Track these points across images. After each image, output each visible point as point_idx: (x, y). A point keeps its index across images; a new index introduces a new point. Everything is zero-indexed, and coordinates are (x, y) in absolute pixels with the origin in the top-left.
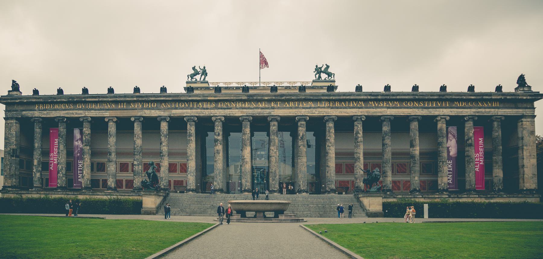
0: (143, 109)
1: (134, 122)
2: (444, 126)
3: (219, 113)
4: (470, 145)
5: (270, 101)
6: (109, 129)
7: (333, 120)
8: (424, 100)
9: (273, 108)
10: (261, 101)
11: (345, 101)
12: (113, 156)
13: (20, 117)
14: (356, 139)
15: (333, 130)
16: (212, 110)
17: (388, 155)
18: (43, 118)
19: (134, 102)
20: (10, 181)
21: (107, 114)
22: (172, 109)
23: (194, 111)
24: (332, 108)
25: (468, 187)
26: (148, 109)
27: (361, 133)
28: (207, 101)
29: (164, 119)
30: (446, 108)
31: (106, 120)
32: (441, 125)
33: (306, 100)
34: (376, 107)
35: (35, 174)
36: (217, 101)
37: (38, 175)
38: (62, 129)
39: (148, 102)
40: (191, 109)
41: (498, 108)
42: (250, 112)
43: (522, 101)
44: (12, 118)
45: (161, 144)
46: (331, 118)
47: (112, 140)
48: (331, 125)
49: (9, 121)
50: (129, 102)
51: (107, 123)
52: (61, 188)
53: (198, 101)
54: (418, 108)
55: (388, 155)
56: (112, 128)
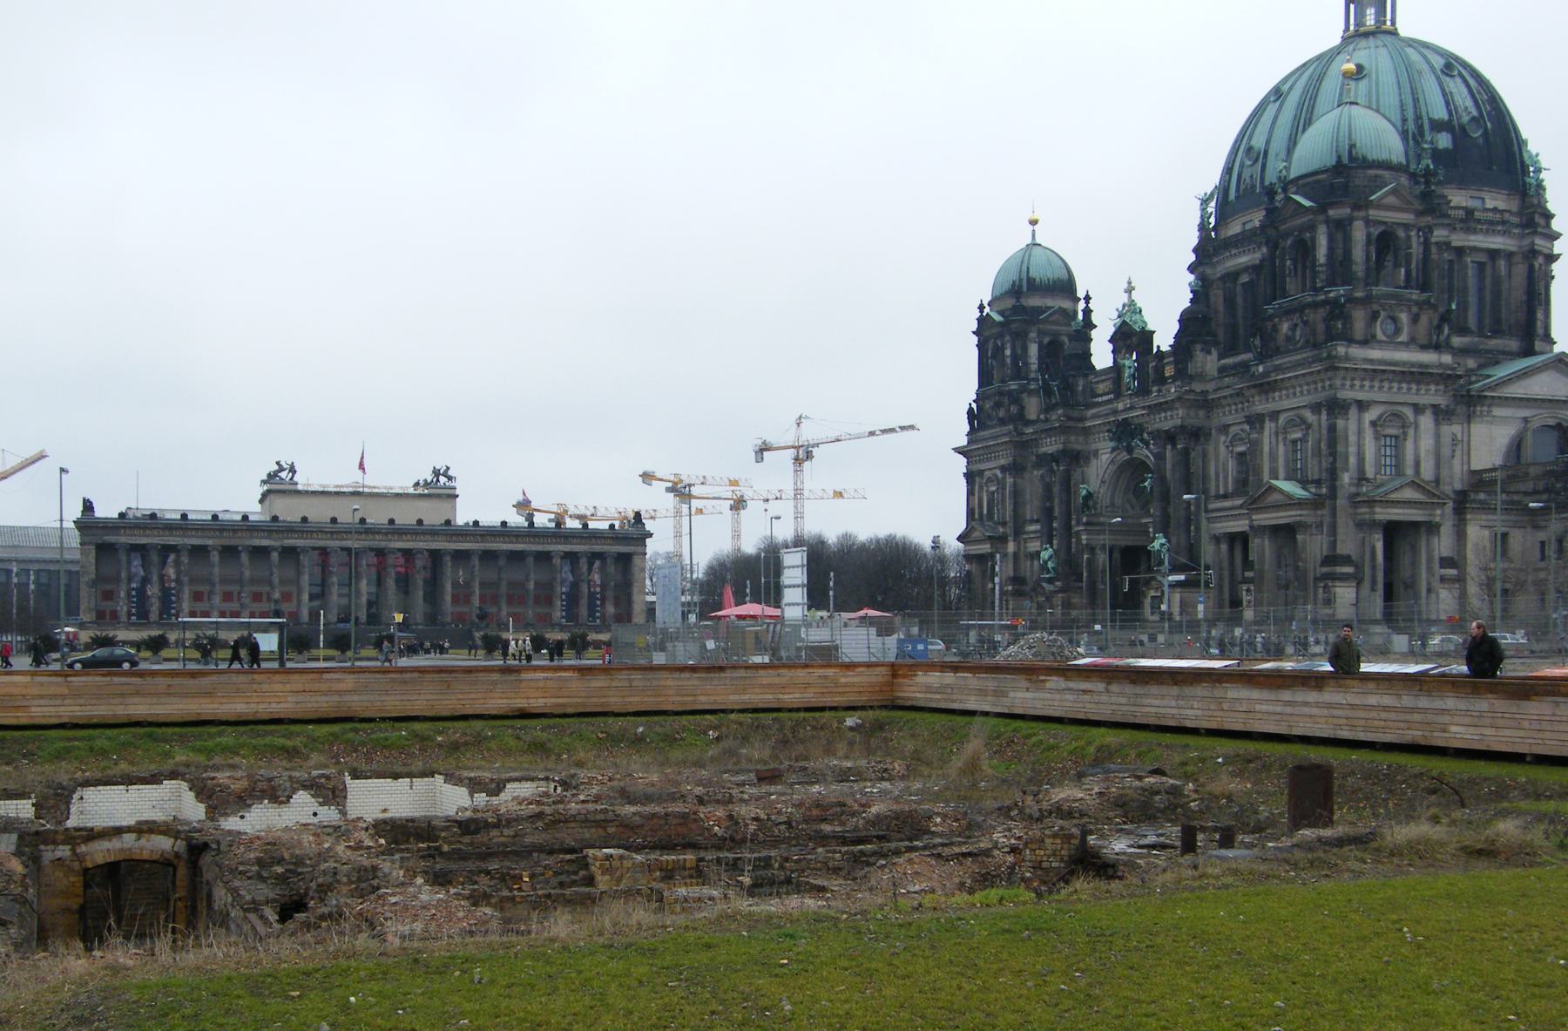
0: (251, 537)
1: (240, 552)
2: (559, 561)
3: (333, 544)
4: (583, 581)
5: (386, 534)
6: (212, 558)
7: (449, 553)
8: (538, 536)
9: (390, 540)
10: (378, 533)
11: (462, 535)
12: (218, 588)
13: (100, 542)
14: (473, 572)
15: (449, 564)
16: (328, 542)
17: (503, 589)
18: (131, 545)
19: (242, 530)
20: (89, 616)
21: (210, 542)
22: (284, 538)
23: (308, 541)
24: (449, 542)
25: (580, 621)
26: (257, 538)
27: (477, 567)
28: (321, 532)
29: (273, 548)
30: (560, 544)
31: (209, 549)
32: (557, 561)
33: (424, 533)
34: (493, 542)
35: (121, 607)
36: (331, 533)
37: (125, 609)
38: (155, 558)
39: (257, 531)
40: (306, 539)
41: (611, 545)
42: (367, 544)
43: (633, 538)
44: (90, 544)
45: (272, 574)
46: (447, 552)
47: (216, 570)
48: (448, 558)
49: (87, 547)
50: (235, 531)
51: (209, 552)
52: (155, 623)
53: (312, 532)
54: (532, 543)
55: (503, 589)
56: (215, 557)
